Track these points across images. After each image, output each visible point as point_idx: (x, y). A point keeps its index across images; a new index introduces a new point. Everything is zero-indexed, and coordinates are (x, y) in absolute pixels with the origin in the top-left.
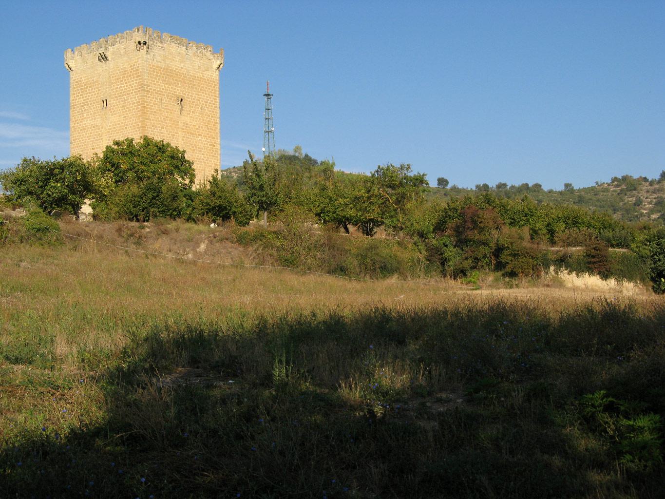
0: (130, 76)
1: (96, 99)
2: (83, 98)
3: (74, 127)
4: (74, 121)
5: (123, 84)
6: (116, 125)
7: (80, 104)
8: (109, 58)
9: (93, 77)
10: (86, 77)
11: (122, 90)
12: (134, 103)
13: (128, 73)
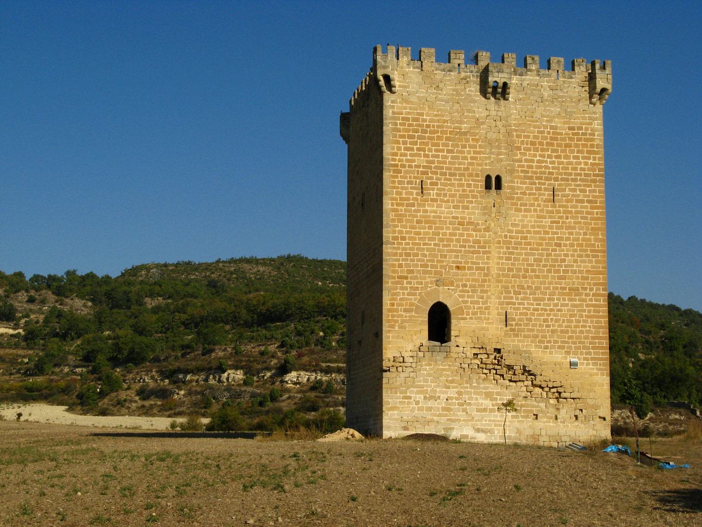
0: (567, 146)
1: (467, 169)
2: (426, 156)
3: (394, 210)
4: (392, 199)
5: (549, 157)
6: (529, 232)
7: (419, 166)
8: (511, 98)
9: (461, 122)
10: (436, 116)
11: (546, 167)
12: (582, 201)
13: (564, 139)
